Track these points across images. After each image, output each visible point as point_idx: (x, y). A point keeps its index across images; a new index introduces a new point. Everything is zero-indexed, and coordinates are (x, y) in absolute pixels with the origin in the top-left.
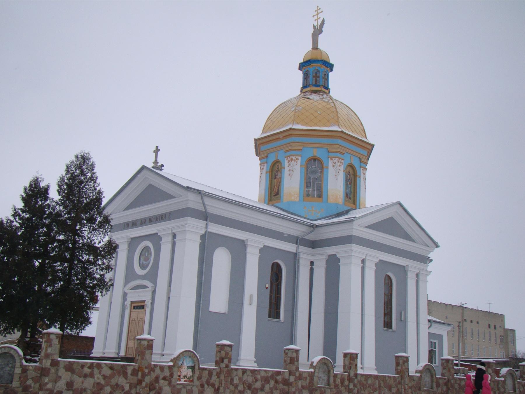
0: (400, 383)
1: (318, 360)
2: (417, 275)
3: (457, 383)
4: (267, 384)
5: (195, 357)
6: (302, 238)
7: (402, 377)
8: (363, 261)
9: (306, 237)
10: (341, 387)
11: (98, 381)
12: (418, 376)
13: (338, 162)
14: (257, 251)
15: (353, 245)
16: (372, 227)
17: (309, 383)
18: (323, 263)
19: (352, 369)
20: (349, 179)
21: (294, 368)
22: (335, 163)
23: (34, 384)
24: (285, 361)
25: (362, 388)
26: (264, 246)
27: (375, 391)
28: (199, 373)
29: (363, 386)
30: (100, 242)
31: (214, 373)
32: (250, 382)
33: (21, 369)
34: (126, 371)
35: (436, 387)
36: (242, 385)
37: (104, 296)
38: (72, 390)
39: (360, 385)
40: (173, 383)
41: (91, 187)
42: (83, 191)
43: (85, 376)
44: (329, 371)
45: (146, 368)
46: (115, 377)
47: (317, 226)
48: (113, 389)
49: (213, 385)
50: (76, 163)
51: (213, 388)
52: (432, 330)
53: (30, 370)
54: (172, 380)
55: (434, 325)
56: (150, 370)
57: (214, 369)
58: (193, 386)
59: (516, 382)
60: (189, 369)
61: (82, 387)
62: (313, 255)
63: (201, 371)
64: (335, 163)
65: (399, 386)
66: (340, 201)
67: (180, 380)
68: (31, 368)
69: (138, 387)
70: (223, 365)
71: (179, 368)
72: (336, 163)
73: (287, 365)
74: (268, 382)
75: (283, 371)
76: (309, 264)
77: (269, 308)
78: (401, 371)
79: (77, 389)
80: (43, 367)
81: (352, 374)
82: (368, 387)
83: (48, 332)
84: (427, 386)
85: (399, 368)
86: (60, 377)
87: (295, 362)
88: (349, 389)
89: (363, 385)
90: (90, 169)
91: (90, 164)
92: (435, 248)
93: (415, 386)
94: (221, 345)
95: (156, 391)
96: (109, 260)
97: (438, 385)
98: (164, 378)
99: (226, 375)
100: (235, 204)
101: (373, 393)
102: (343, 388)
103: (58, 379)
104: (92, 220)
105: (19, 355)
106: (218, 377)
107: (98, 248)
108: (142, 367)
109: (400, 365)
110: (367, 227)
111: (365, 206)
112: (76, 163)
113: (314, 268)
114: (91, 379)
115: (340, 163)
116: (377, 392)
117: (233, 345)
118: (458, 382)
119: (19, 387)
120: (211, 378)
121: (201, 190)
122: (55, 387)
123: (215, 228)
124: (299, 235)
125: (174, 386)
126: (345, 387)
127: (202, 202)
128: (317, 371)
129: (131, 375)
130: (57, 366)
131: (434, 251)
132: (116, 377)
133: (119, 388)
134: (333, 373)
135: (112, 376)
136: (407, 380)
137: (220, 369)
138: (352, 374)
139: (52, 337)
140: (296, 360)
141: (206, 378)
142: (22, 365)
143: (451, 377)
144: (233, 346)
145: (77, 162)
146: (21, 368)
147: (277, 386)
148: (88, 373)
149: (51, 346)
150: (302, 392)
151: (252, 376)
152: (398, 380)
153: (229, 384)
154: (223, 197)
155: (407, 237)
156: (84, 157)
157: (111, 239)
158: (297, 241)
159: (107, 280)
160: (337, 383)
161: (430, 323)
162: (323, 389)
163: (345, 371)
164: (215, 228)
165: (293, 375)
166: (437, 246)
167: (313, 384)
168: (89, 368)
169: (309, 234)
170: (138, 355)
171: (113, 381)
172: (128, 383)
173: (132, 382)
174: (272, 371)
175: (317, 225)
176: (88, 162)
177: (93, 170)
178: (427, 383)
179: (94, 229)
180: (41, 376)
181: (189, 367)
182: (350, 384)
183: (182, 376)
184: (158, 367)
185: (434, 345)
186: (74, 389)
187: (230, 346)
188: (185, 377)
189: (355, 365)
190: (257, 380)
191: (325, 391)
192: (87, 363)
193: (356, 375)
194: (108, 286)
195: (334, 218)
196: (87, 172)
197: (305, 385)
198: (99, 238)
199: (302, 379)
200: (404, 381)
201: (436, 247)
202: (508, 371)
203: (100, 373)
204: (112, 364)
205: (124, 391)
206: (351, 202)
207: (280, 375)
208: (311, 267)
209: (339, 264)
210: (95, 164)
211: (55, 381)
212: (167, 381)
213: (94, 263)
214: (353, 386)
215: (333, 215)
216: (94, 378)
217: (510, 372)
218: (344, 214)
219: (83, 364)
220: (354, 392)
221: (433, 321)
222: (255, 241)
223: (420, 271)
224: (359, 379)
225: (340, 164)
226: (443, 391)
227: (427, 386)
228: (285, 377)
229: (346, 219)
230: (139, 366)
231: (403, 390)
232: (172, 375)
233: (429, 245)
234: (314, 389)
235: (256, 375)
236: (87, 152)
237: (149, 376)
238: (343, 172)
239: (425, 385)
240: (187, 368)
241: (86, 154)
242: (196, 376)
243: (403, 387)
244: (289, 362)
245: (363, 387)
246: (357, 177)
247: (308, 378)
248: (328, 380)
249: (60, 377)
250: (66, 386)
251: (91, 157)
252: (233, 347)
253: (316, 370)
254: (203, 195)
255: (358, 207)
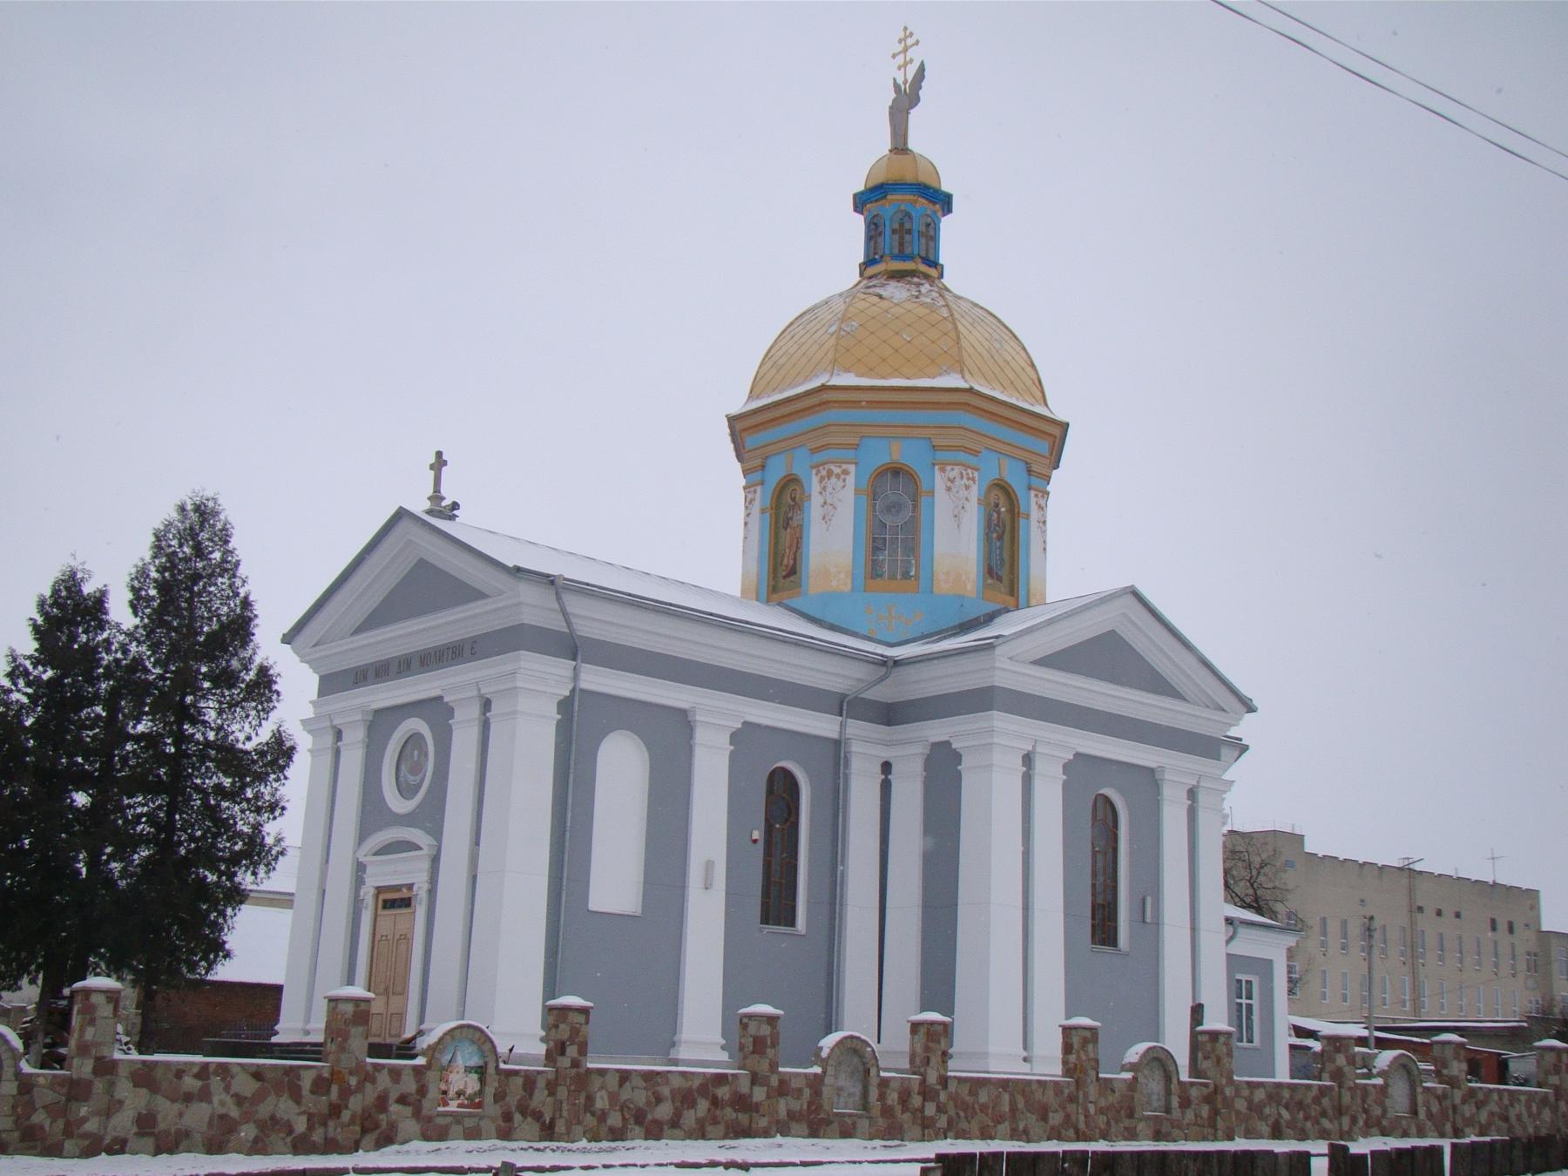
0: (1072, 1099)
1: (834, 1043)
2: (1192, 794)
3: (1241, 1097)
4: (688, 1108)
5: (485, 1042)
6: (856, 697)
7: (1079, 1084)
8: (1028, 759)
9: (867, 695)
10: (899, 1115)
11: (222, 1111)
12: (1125, 1080)
13: (962, 478)
14: (725, 740)
15: (995, 713)
16: (1058, 661)
17: (810, 1104)
18: (918, 766)
19: (931, 1065)
20: (997, 525)
21: (763, 1066)
22: (952, 481)
23: (51, 1123)
24: (742, 1047)
25: (962, 1114)
26: (745, 724)
27: (999, 1123)
28: (499, 1082)
29: (965, 1111)
30: (249, 738)
31: (541, 1083)
32: (641, 1106)
33: (17, 1083)
34: (296, 1081)
35: (1180, 1107)
36: (619, 1114)
37: (262, 883)
38: (152, 1134)
39: (956, 1107)
40: (425, 1112)
41: (223, 590)
42: (202, 602)
43: (188, 1098)
44: (867, 1072)
45: (351, 1073)
46: (269, 1098)
47: (897, 663)
48: (262, 1131)
49: (538, 1116)
50: (180, 525)
51: (538, 1121)
52: (1238, 948)
53: (39, 1086)
54: (423, 1103)
55: (1243, 932)
56: (363, 1078)
57: (539, 1072)
58: (482, 1118)
59: (1419, 1090)
60: (471, 1075)
61: (179, 1127)
62: (888, 744)
63: (503, 1077)
64: (952, 481)
65: (1071, 1108)
66: (969, 587)
67: (446, 1104)
68: (41, 1080)
69: (331, 1124)
70: (565, 1062)
71: (444, 1072)
72: (957, 479)
73: (745, 1058)
74: (692, 1104)
75: (733, 1075)
76: (878, 769)
77: (762, 898)
78: (1076, 1065)
79: (167, 1132)
80: (75, 1077)
81: (932, 1078)
82: (978, 1111)
83: (84, 987)
84: (1155, 1104)
85: (1072, 1058)
86: (121, 1102)
87: (768, 1050)
88: (923, 1118)
89: (965, 1107)
90: (220, 539)
91: (219, 526)
92: (1243, 715)
93: (1116, 1105)
94: (559, 1009)
95: (381, 1133)
96: (274, 786)
97: (1185, 1103)
98: (402, 1100)
99: (573, 1088)
100: (653, 610)
101: (995, 1126)
102: (907, 1116)
103: (113, 1107)
104: (225, 679)
105: (13, 1050)
106: (552, 1093)
107: (247, 753)
108: (339, 1072)
109: (1074, 1051)
110: (1035, 663)
111: (1045, 599)
112: (180, 525)
113: (892, 781)
114: (204, 1105)
115: (968, 479)
116: (1007, 1123)
117: (592, 1008)
118: (1246, 1092)
119: (12, 1131)
120: (531, 1095)
121: (554, 576)
122: (106, 1128)
123: (598, 679)
124: (849, 690)
125: (430, 1119)
126: (912, 1113)
127: (559, 609)
128: (830, 1071)
129: (312, 1092)
130: (112, 1074)
131: (1241, 722)
132: (271, 1099)
133: (277, 1127)
134: (878, 1075)
135: (259, 1097)
136: (1092, 1090)
137: (557, 1071)
138: (932, 1078)
139: (95, 999)
140: (769, 1043)
141: (518, 1097)
142: (18, 1074)
143: (1224, 1081)
144: (591, 1010)
145: (183, 522)
146: (16, 1080)
147: (718, 1112)
148: (196, 1091)
149: (92, 1022)
150: (789, 1128)
151: (645, 1088)
152: (1066, 1091)
153: (582, 1112)
154: (619, 592)
155: (1158, 684)
156: (203, 508)
157: (280, 726)
158: (842, 705)
159: (269, 840)
160: (889, 1102)
161: (1231, 929)
162: (849, 1121)
163: (916, 1069)
164: (598, 679)
165: (761, 1085)
166: (1251, 709)
167: (819, 1108)
168: (197, 1076)
169: (878, 686)
170: (329, 1040)
171: (264, 1110)
172: (303, 1113)
173: (316, 1111)
174: (704, 1074)
175: (896, 659)
176: (214, 521)
177: (227, 542)
178: (1155, 1097)
179: (233, 705)
180: (68, 1100)
181: (472, 1068)
182: (926, 1104)
183: (452, 1093)
184: (386, 1070)
185: (1246, 989)
186: (159, 1132)
187: (584, 1011)
188: (459, 1094)
189: (940, 1053)
190: (659, 1100)
191: (854, 1124)
192: (193, 1064)
193: (944, 1081)
194: (272, 855)
195: (954, 635)
196: (210, 549)
197: (797, 1108)
198: (247, 726)
199: (787, 1095)
200: (1086, 1095)
201: (1247, 712)
202: (1396, 1058)
203: (227, 1089)
204: (258, 1066)
205: (294, 1135)
206: (1003, 589)
207: (725, 1085)
208: (883, 777)
209: (959, 768)
210: (232, 528)
211: (107, 1114)
212: (411, 1108)
213: (234, 795)
214: (935, 1110)
215: (947, 630)
216: (210, 1102)
217: (1401, 1062)
218: (981, 624)
219: (180, 1067)
220: (938, 1125)
221: (1241, 923)
222: (718, 710)
223: (1198, 782)
224: (954, 1091)
225: (967, 483)
226: (1199, 1119)
227: (1155, 1104)
228: (738, 1089)
229: (975, 641)
230: (333, 1069)
231: (1082, 1118)
232: (422, 1091)
233: (1225, 708)
234: (823, 1119)
235: (659, 1085)
236: (209, 493)
237: (360, 1096)
238: (976, 504)
239: (1149, 1102)
240: (465, 1071)
241: (208, 500)
242: (490, 1091)
243: (1080, 1111)
244: (751, 1048)
245: (966, 1114)
246: (1019, 517)
247: (807, 1093)
248: (865, 1094)
249: (121, 1102)
250: (135, 1125)
251: (221, 508)
252: (591, 1014)
253: (829, 1068)
254: (562, 588)
255: (1022, 602)
